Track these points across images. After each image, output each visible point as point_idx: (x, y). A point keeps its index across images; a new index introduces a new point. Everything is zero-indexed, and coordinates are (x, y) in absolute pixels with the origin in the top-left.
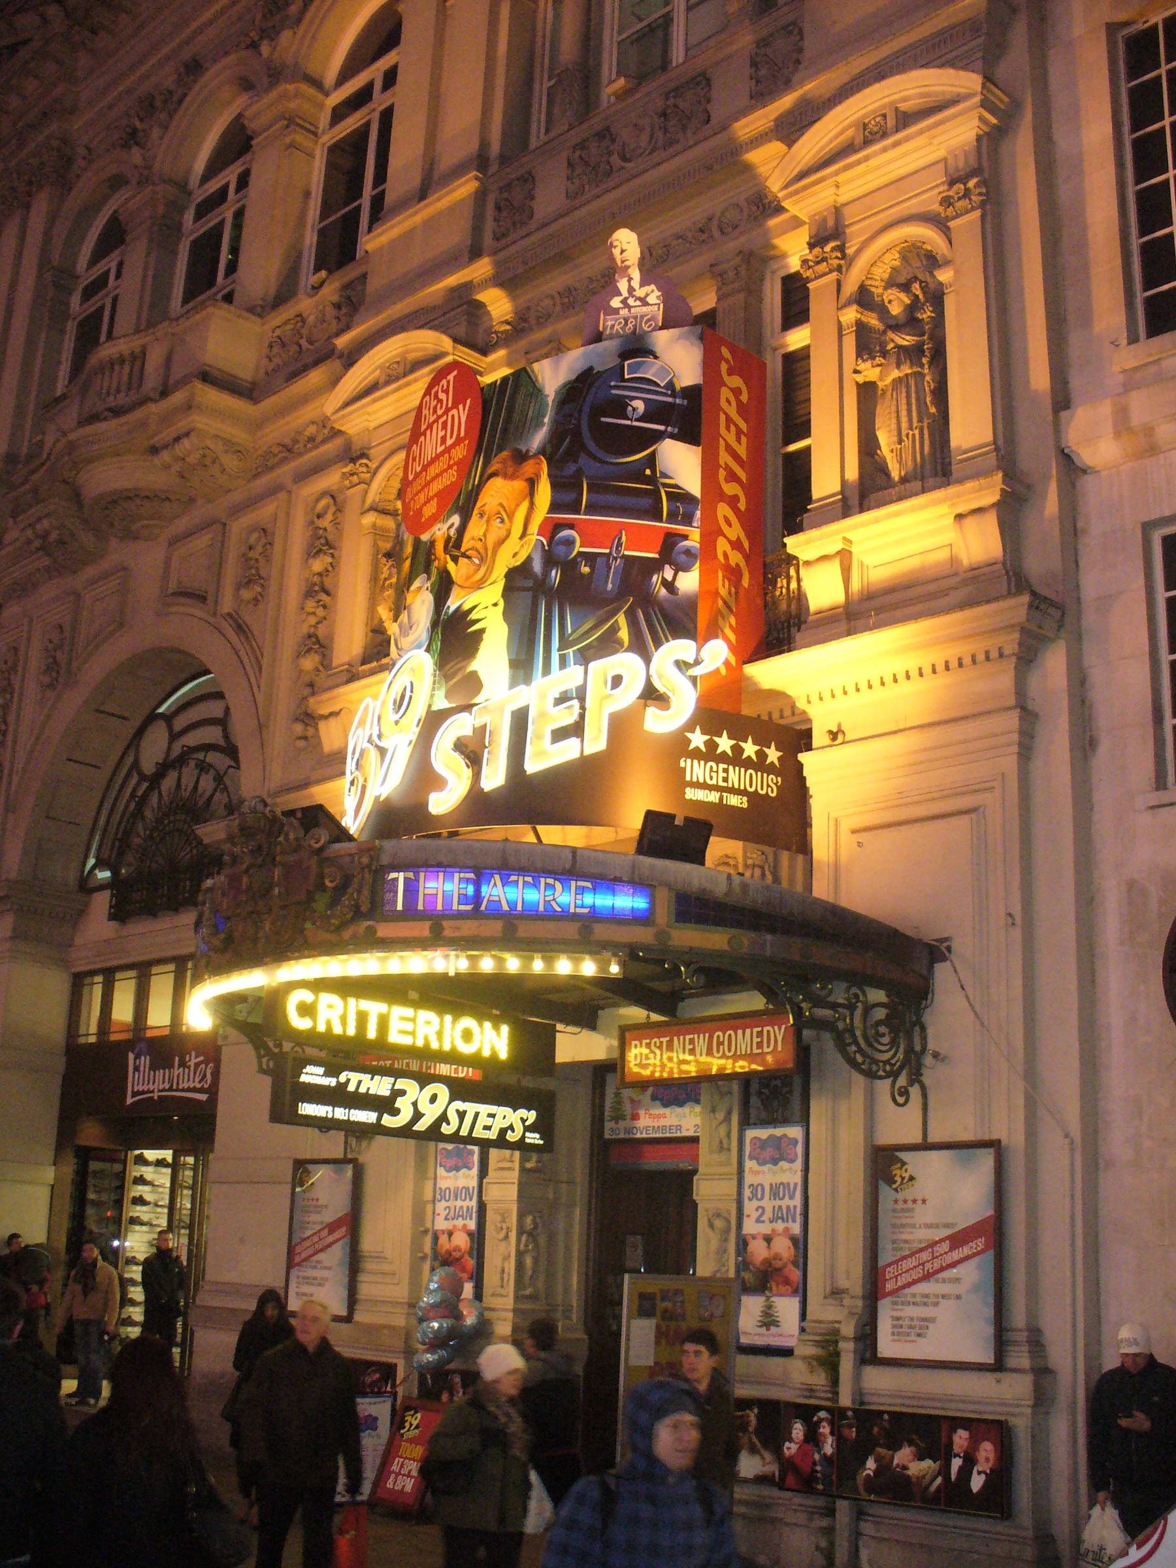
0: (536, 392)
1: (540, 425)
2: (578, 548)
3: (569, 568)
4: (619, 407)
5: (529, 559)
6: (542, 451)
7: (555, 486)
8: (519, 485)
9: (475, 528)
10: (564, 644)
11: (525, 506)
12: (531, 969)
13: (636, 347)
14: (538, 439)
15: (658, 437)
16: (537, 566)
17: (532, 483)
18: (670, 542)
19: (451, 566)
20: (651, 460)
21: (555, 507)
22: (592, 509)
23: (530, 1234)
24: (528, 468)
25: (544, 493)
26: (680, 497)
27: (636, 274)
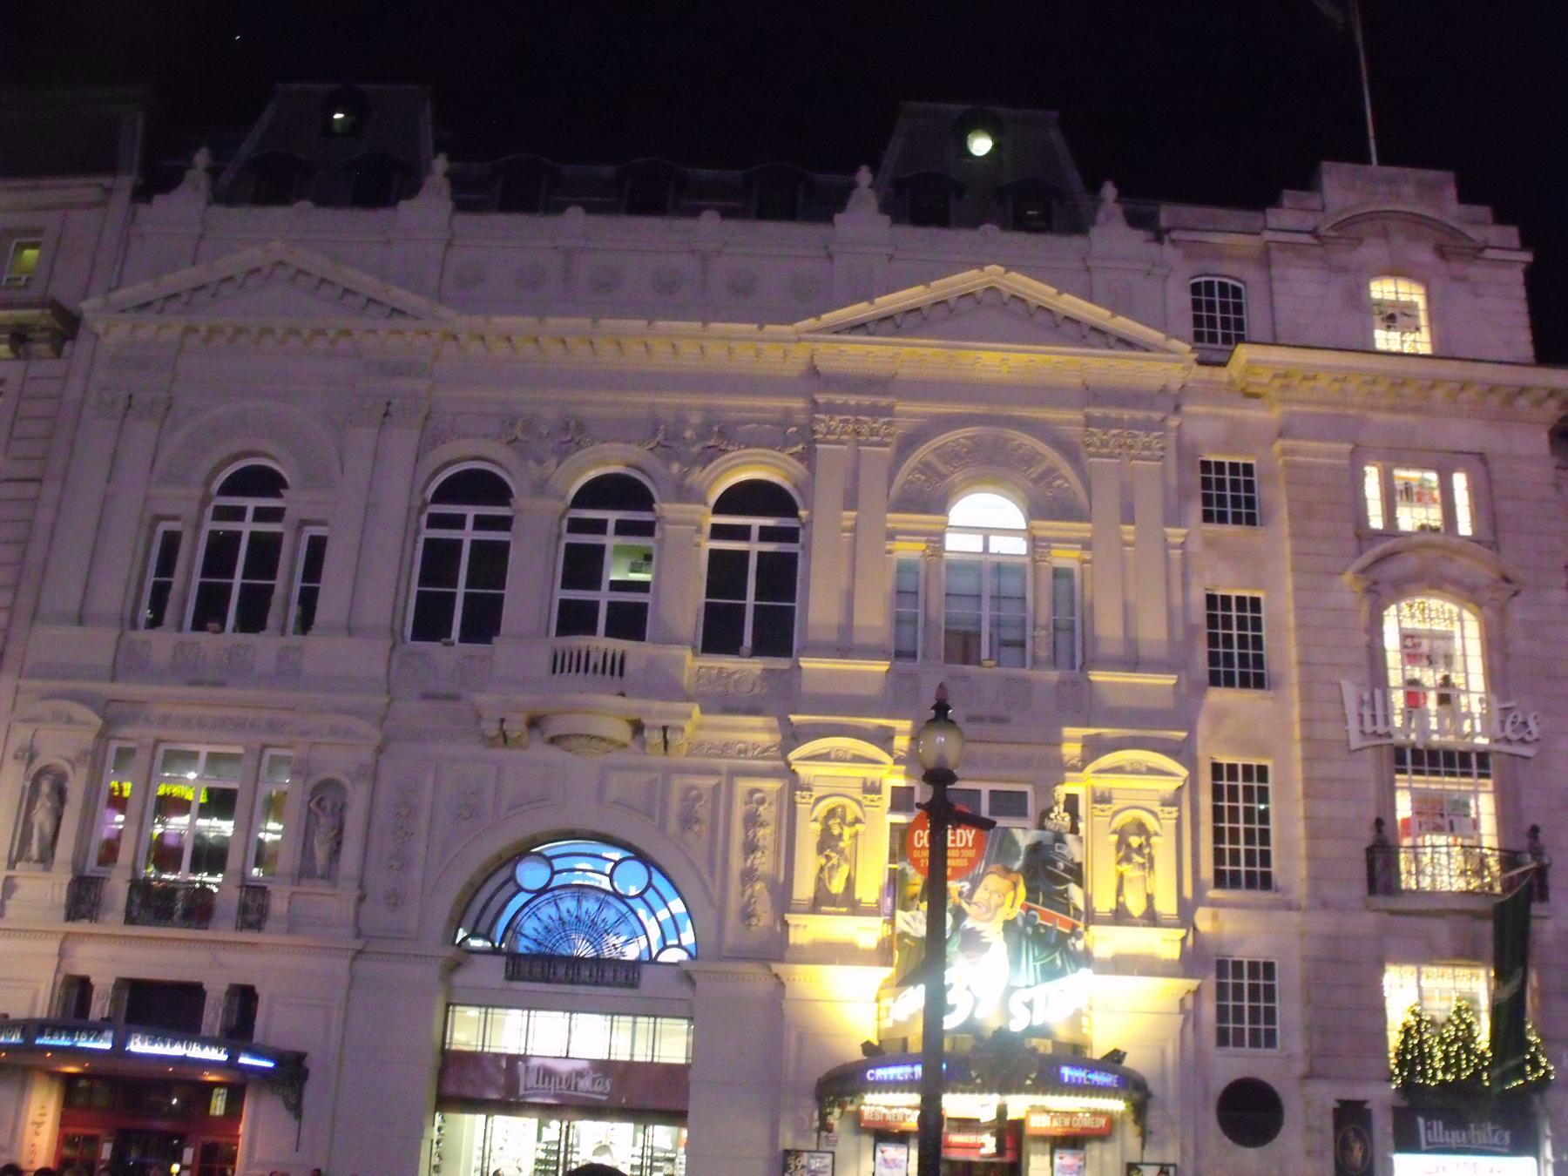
0: (1014, 843)
1: (1017, 859)
2: (1039, 921)
3: (1036, 927)
4: (1054, 863)
5: (1015, 920)
6: (1018, 872)
7: (1029, 890)
8: (1007, 883)
9: (980, 895)
10: (1035, 959)
11: (1012, 894)
12: (1123, 1114)
13: (1059, 838)
14: (1018, 865)
15: (1068, 881)
16: (1020, 922)
17: (1015, 886)
18: (1074, 927)
19: (965, 905)
20: (1066, 890)
21: (1027, 899)
22: (1044, 905)
23: (28, 1048)
24: (1013, 876)
25: (1022, 890)
26: (1076, 909)
27: (1062, 807)
